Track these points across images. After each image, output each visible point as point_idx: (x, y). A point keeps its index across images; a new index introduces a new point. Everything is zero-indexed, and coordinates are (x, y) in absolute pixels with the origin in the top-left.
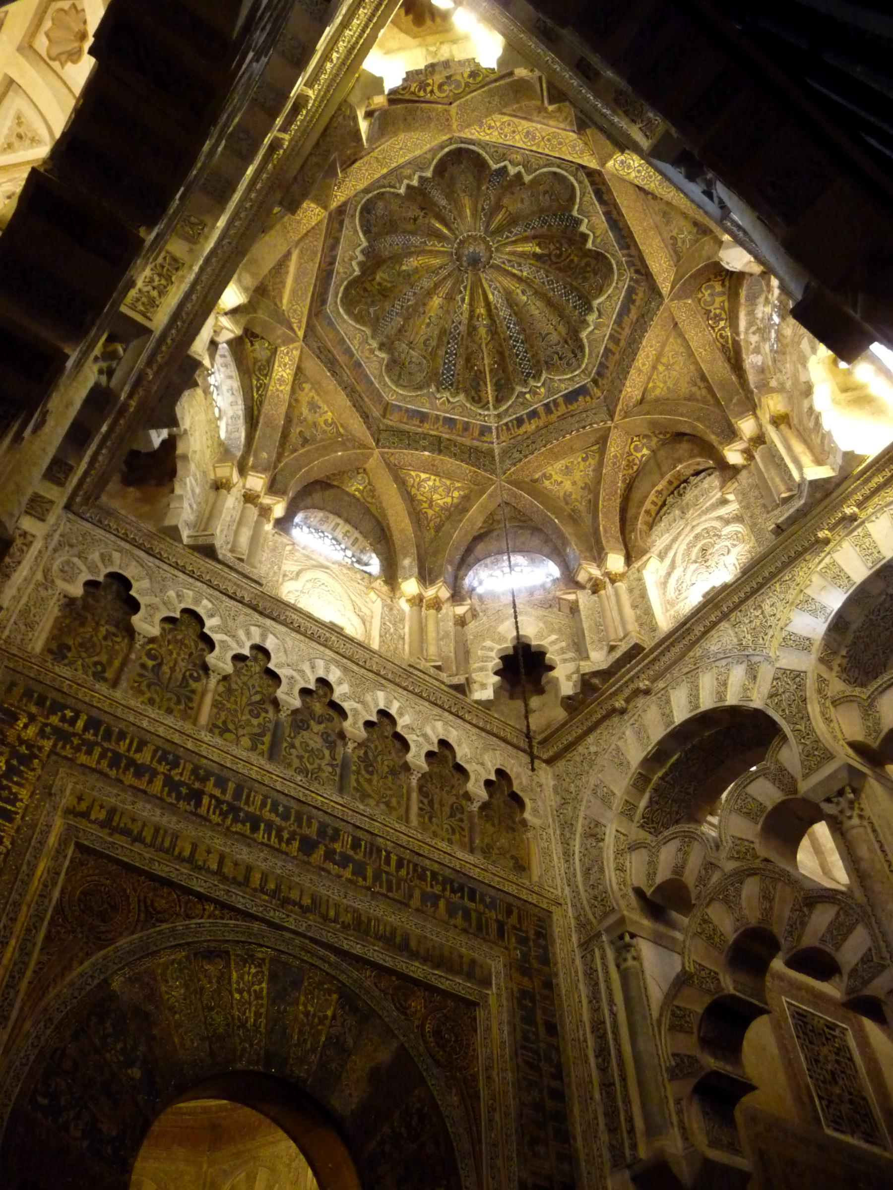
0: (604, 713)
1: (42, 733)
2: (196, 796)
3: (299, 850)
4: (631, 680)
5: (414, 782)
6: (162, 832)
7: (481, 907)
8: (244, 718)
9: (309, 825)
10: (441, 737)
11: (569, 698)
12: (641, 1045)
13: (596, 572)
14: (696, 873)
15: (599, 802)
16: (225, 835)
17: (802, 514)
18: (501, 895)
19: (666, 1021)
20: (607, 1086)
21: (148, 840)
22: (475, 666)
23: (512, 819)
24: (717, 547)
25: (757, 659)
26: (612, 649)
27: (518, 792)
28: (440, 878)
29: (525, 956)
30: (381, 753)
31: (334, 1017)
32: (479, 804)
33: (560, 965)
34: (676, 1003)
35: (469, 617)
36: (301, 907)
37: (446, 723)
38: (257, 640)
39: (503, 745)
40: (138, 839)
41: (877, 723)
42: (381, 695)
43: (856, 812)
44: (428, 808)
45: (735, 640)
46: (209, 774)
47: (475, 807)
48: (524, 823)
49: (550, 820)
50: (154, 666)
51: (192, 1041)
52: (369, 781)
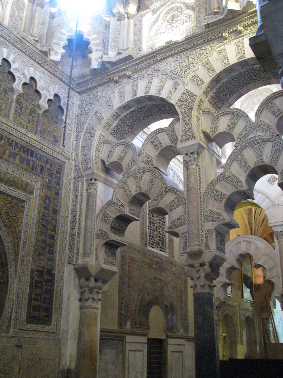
0: (108, 80)
4: (124, 69)
5: (15, 97)
7: (35, 159)
10: (32, 76)
11: (95, 69)
12: (88, 223)
13: (122, 10)
14: (127, 163)
15: (96, 119)
17: (220, 22)
18: (45, 154)
19: (100, 217)
20: (72, 235)
22: (55, 41)
23: (57, 117)
24: (179, 18)
25: (179, 81)
26: (119, 53)
27: (62, 106)
28: (19, 146)
32: (43, 110)
33: (64, 186)
34: (106, 211)
35: (57, 14)
37: (35, 69)
39: (60, 82)
41: (216, 128)
42: (5, 50)
43: (196, 163)
44: (19, 111)
45: (173, 68)
47: (41, 112)
49: (74, 121)
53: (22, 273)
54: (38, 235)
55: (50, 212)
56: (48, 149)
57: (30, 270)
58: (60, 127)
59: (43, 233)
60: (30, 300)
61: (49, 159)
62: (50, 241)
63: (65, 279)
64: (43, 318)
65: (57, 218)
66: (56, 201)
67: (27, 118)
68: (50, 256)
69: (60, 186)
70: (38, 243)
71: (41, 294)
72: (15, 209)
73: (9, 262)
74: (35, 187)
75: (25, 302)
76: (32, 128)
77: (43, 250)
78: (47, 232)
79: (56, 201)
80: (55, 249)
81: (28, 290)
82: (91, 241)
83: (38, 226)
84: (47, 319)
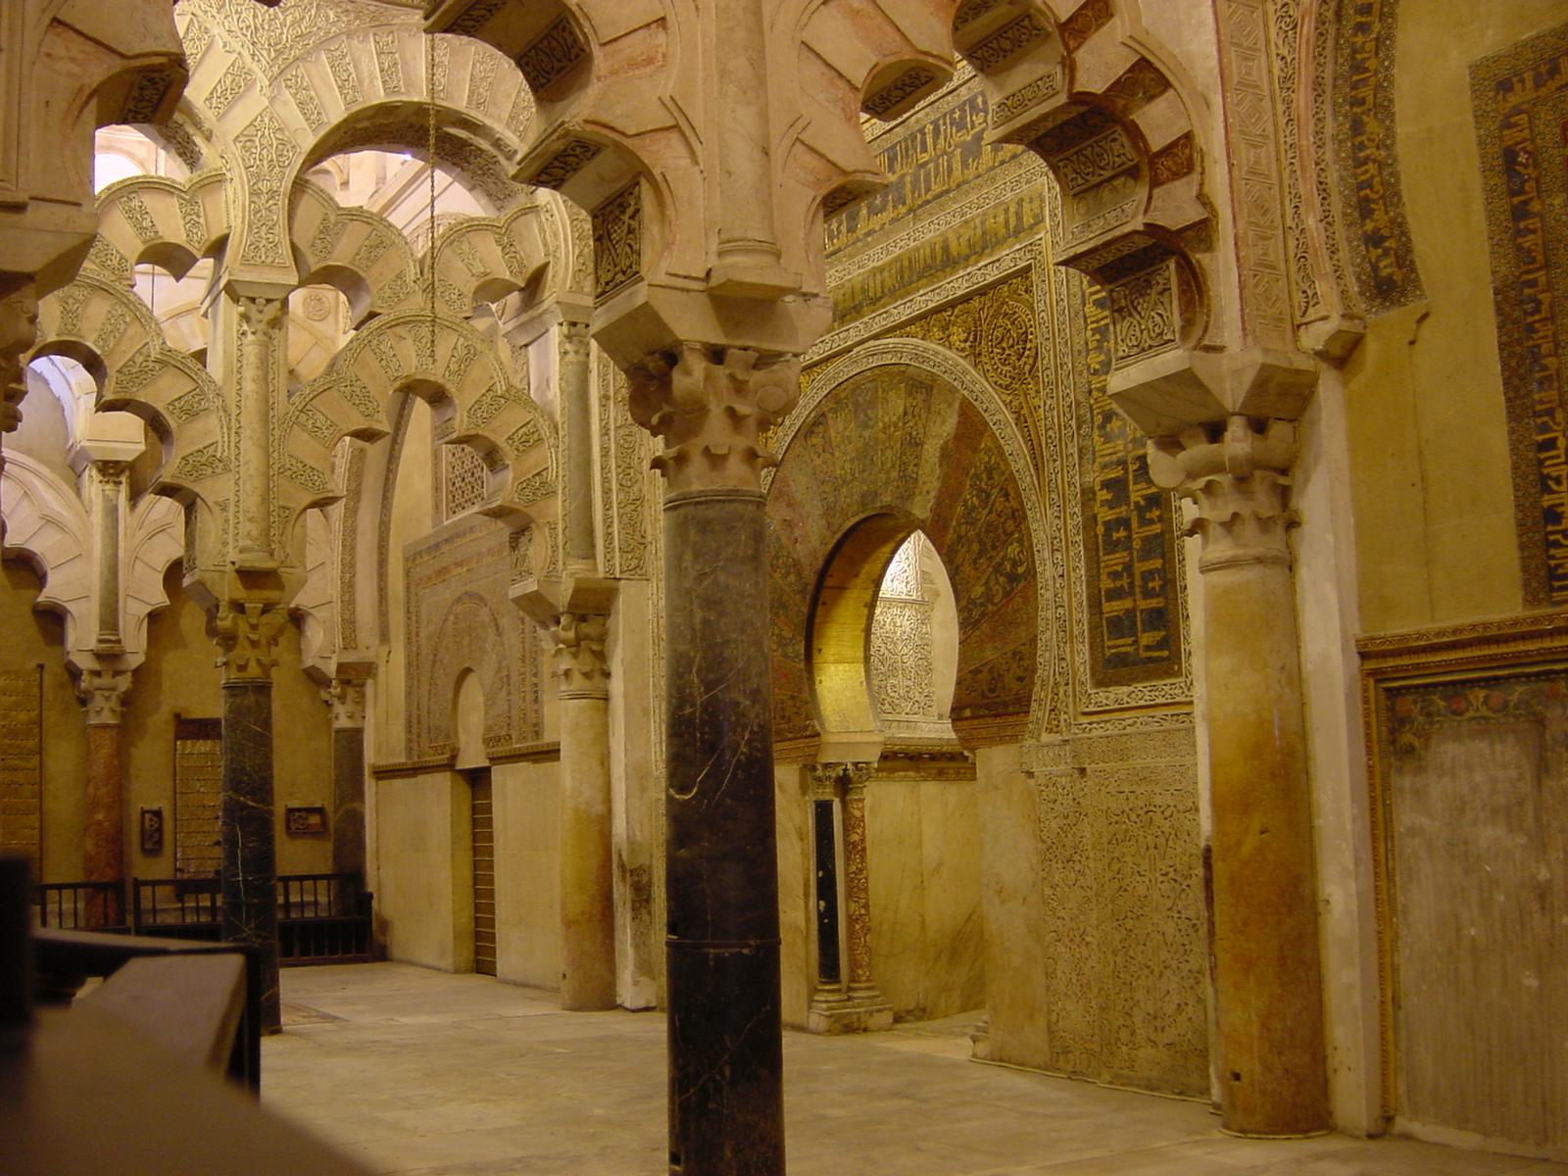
3: (848, 231)
31: (905, 413)
60: (1095, 604)
64: (1149, 654)
81: (1083, 572)
83: (1085, 318)
84: (1166, 653)
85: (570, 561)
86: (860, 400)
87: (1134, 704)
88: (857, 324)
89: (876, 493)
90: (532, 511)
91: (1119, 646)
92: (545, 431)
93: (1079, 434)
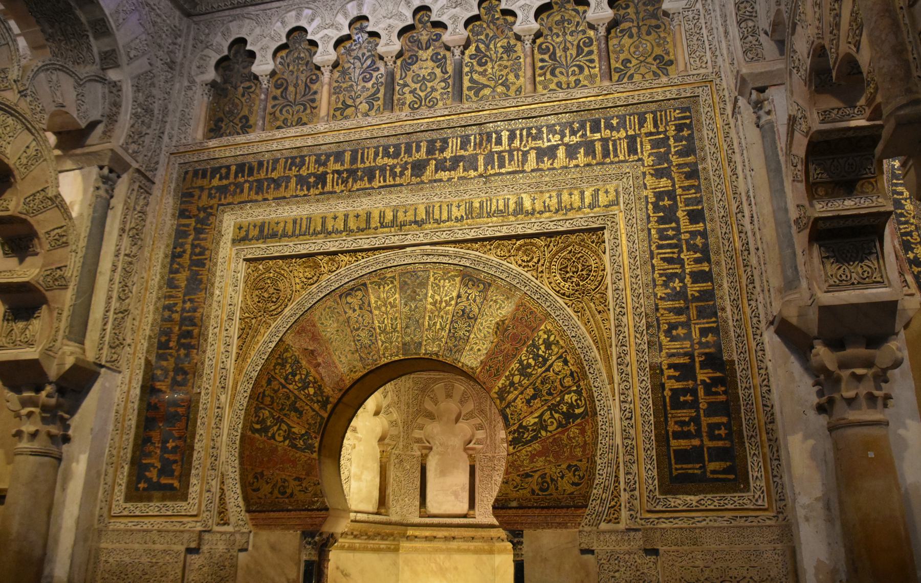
1: (210, 196)
2: (321, 179)
3: (411, 176)
5: (528, 46)
6: (298, 221)
7: (606, 133)
8: (359, 88)
9: (418, 150)
16: (349, 197)
21: (290, 233)
28: (558, 128)
29: (663, 158)
30: (495, 37)
31: (459, 296)
32: (605, 26)
33: (707, 148)
34: (794, 152)
36: (416, 222)
38: (354, 13)
40: (285, 235)
46: (328, 156)
47: (602, 31)
48: (666, 14)
50: (282, 93)
51: (346, 356)
52: (483, 73)
53: (625, 383)
54: (655, 285)
55: (681, 223)
56: (637, 93)
57: (648, 369)
58: (670, 29)
59: (670, 277)
60: (662, 439)
61: (646, 113)
62: (698, 289)
63: (769, 364)
64: (715, 476)
65: (705, 229)
66: (693, 191)
67: (575, 65)
68: (708, 323)
69: (695, 155)
70: (662, 304)
71: (696, 420)
72: (581, 254)
73: (587, 368)
74: (620, 189)
75: (648, 446)
76: (592, 77)
77: (682, 315)
78: (684, 271)
79: (693, 191)
80: (719, 302)
81: (652, 418)
82: (792, 246)
83: (653, 266)
84: (732, 477)
85: (65, 341)
86: (409, 282)
87: (703, 507)
88: (418, 233)
89: (420, 343)
90: (48, 294)
91: (686, 469)
92: (71, 238)
93: (647, 333)
